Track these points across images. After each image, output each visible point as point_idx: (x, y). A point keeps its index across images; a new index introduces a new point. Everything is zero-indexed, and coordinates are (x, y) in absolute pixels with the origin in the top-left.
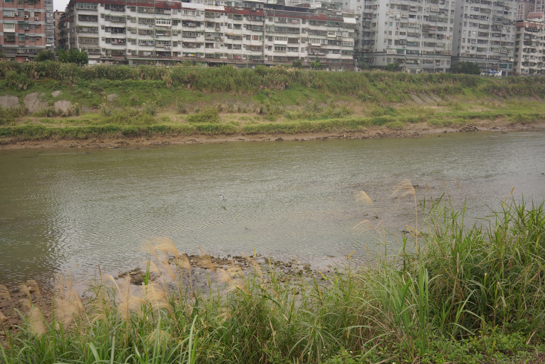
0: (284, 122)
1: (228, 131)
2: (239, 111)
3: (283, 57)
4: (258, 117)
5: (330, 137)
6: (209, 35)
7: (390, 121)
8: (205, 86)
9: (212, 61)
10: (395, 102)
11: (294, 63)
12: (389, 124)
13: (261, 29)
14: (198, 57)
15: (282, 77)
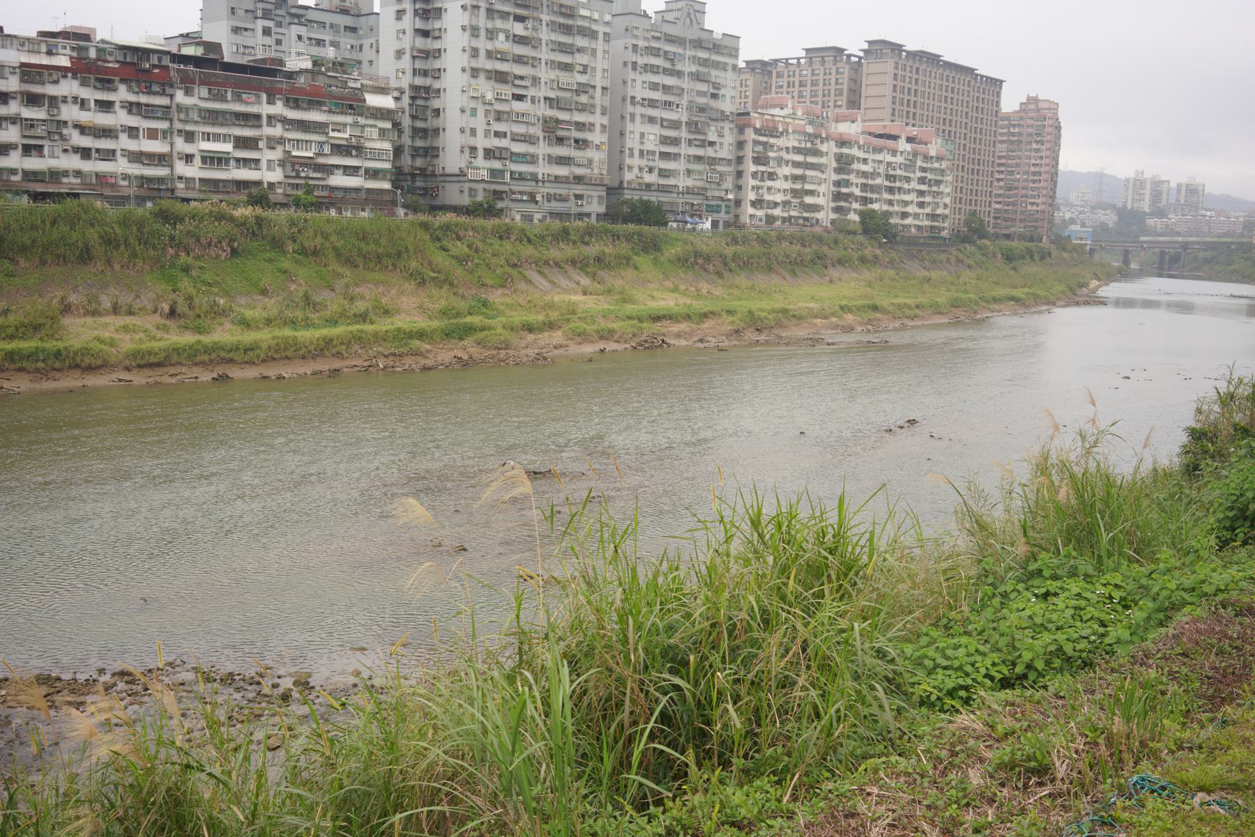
0: (232, 335)
1: (87, 361)
2: (115, 310)
3: (224, 181)
4: (165, 325)
5: (345, 370)
6: (32, 126)
7: (483, 329)
8: (23, 249)
9: (40, 188)
10: (492, 287)
11: (250, 195)
12: (481, 335)
13: (165, 113)
14: (5, 177)
15: (223, 229)
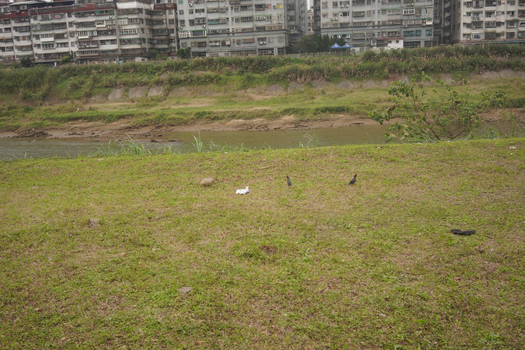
13: (29, 29)
